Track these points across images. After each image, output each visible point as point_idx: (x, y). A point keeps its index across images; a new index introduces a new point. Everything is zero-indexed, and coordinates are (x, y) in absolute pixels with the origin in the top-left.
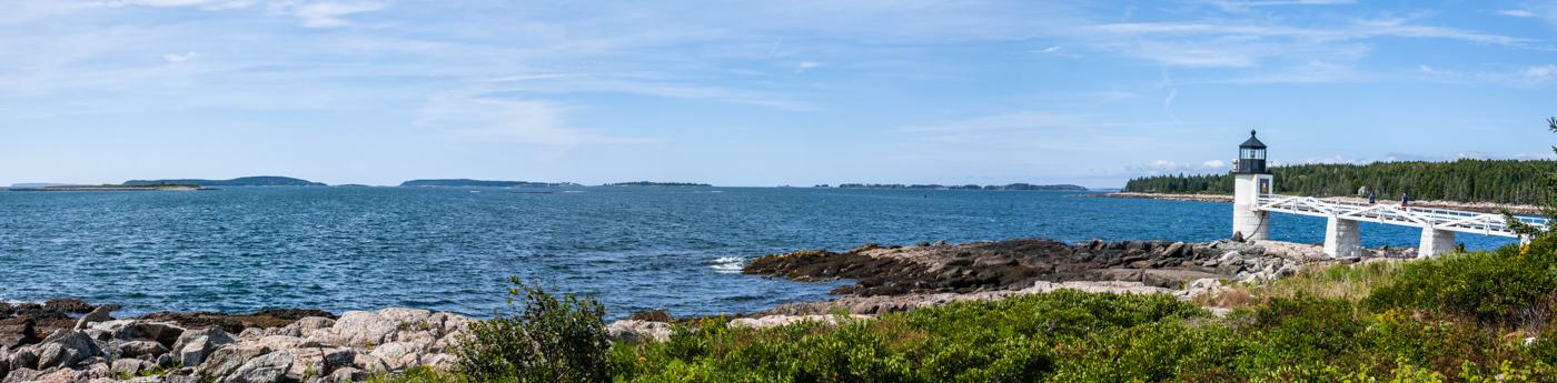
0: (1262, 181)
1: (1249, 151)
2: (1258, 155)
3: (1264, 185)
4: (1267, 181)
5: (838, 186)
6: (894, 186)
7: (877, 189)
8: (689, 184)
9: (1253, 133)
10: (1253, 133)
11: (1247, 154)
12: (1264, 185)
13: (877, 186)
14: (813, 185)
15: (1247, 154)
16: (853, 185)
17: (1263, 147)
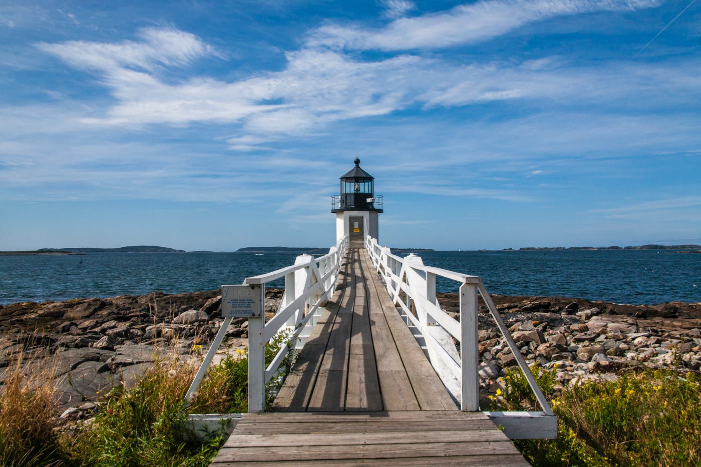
0: (352, 220)
1: (353, 184)
2: (364, 188)
3: (356, 225)
4: (360, 220)
5: (518, 249)
6: (558, 248)
7: (546, 251)
8: (420, 249)
9: (357, 162)
10: (357, 162)
11: (351, 188)
12: (356, 225)
13: (546, 248)
14: (478, 250)
15: (351, 188)
16: (529, 249)
17: (369, 179)
